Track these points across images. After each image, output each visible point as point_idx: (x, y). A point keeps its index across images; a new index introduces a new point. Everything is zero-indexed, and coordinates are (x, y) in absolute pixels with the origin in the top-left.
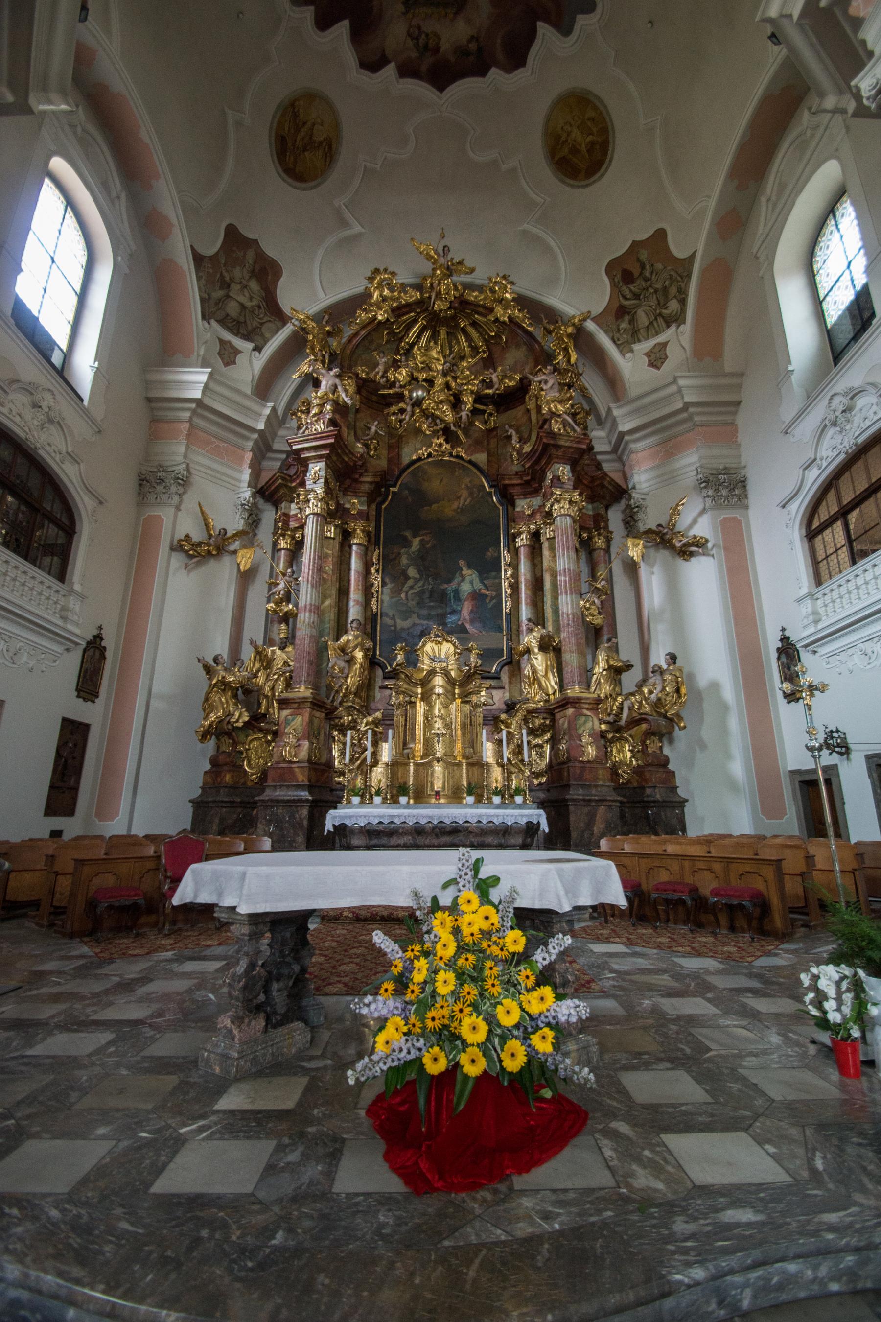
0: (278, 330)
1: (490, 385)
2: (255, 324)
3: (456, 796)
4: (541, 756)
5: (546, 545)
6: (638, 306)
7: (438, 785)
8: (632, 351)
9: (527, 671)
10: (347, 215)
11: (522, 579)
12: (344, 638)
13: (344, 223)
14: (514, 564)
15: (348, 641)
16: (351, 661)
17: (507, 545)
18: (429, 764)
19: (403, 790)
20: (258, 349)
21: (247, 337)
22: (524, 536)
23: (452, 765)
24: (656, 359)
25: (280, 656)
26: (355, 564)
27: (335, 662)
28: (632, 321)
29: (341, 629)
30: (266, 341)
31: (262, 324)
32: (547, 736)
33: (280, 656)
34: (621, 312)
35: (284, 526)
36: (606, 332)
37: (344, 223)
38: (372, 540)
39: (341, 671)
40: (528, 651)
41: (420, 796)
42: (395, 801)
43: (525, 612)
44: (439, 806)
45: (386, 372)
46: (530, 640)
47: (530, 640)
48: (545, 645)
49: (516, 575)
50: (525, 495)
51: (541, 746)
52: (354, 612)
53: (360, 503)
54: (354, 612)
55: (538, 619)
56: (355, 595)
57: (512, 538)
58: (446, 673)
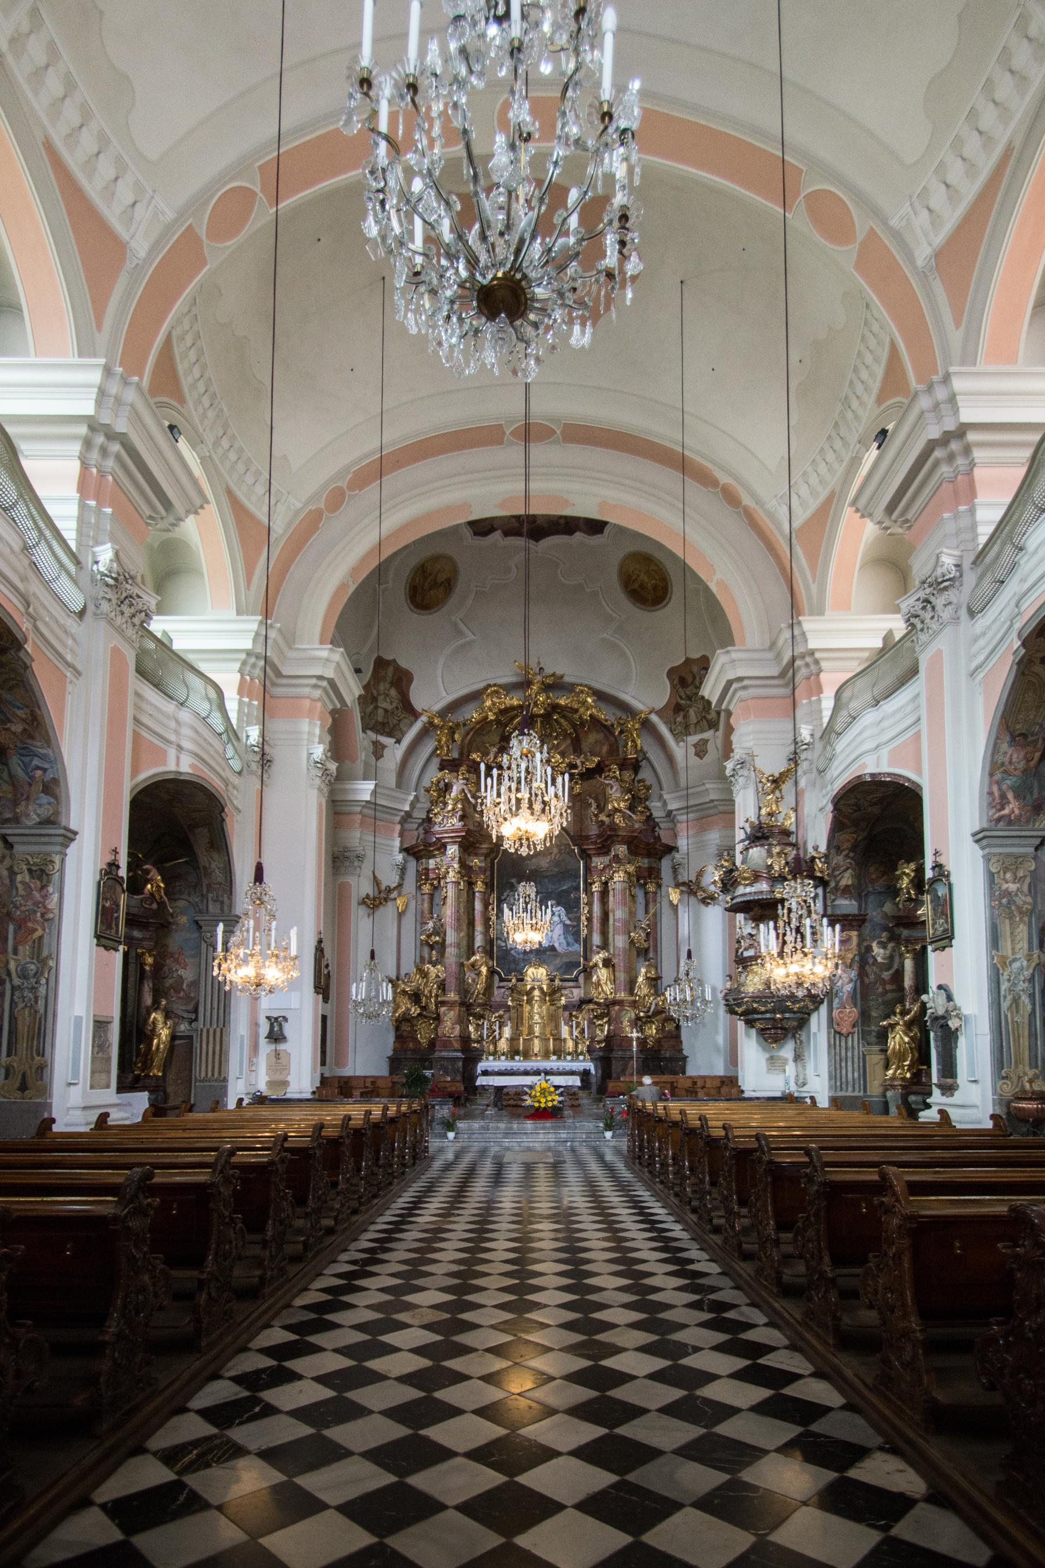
0: (411, 725)
1: (575, 767)
2: (395, 722)
3: (546, 1055)
4: (602, 1031)
5: (611, 893)
6: (690, 706)
7: (536, 1050)
8: (683, 741)
9: (595, 978)
10: (462, 626)
11: (595, 915)
12: (473, 959)
13: (460, 633)
14: (590, 904)
15: (476, 960)
16: (479, 974)
17: (586, 891)
18: (531, 1039)
19: (517, 1052)
20: (398, 742)
21: (390, 735)
22: (596, 884)
23: (544, 1040)
24: (701, 750)
25: (433, 971)
26: (478, 906)
27: (470, 977)
28: (685, 717)
29: (471, 951)
30: (403, 734)
31: (400, 721)
32: (605, 1020)
33: (433, 971)
34: (678, 709)
35: (427, 878)
36: (665, 723)
37: (460, 633)
38: (489, 886)
39: (473, 980)
40: (596, 965)
41: (527, 1055)
42: (513, 1058)
43: (596, 939)
44: (537, 1061)
45: (495, 757)
46: (598, 958)
47: (598, 958)
48: (607, 963)
49: (590, 912)
50: (599, 855)
51: (602, 1025)
52: (479, 941)
53: (480, 862)
54: (479, 941)
55: (605, 946)
56: (479, 928)
57: (588, 885)
58: (541, 989)
